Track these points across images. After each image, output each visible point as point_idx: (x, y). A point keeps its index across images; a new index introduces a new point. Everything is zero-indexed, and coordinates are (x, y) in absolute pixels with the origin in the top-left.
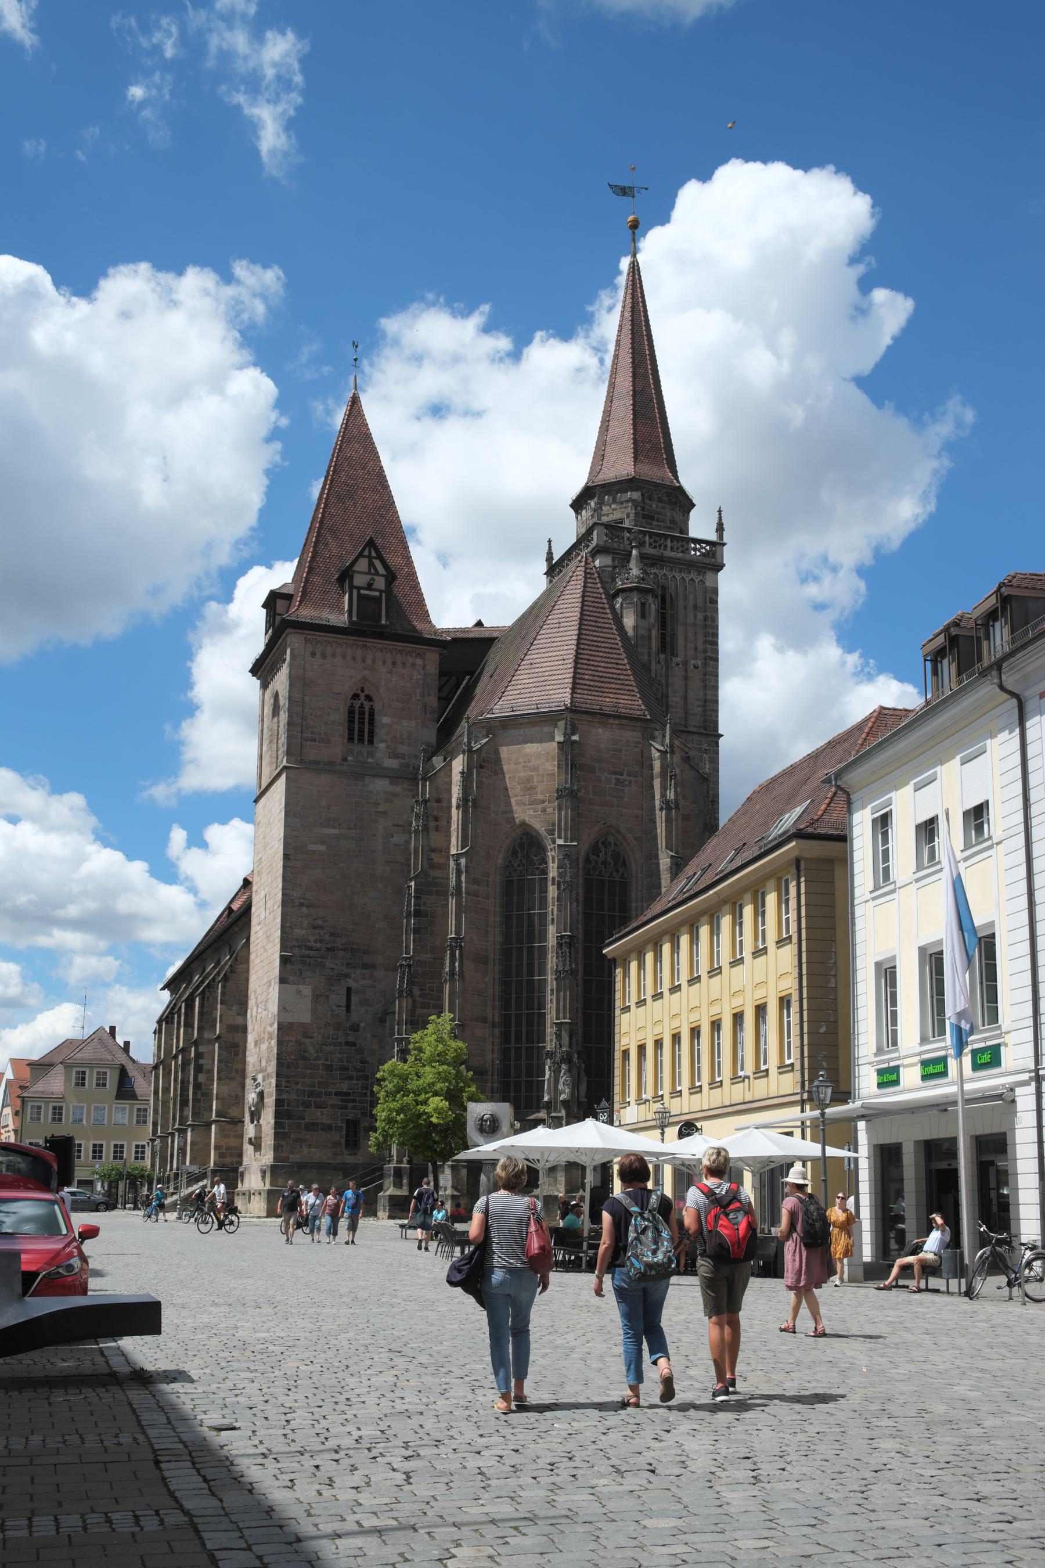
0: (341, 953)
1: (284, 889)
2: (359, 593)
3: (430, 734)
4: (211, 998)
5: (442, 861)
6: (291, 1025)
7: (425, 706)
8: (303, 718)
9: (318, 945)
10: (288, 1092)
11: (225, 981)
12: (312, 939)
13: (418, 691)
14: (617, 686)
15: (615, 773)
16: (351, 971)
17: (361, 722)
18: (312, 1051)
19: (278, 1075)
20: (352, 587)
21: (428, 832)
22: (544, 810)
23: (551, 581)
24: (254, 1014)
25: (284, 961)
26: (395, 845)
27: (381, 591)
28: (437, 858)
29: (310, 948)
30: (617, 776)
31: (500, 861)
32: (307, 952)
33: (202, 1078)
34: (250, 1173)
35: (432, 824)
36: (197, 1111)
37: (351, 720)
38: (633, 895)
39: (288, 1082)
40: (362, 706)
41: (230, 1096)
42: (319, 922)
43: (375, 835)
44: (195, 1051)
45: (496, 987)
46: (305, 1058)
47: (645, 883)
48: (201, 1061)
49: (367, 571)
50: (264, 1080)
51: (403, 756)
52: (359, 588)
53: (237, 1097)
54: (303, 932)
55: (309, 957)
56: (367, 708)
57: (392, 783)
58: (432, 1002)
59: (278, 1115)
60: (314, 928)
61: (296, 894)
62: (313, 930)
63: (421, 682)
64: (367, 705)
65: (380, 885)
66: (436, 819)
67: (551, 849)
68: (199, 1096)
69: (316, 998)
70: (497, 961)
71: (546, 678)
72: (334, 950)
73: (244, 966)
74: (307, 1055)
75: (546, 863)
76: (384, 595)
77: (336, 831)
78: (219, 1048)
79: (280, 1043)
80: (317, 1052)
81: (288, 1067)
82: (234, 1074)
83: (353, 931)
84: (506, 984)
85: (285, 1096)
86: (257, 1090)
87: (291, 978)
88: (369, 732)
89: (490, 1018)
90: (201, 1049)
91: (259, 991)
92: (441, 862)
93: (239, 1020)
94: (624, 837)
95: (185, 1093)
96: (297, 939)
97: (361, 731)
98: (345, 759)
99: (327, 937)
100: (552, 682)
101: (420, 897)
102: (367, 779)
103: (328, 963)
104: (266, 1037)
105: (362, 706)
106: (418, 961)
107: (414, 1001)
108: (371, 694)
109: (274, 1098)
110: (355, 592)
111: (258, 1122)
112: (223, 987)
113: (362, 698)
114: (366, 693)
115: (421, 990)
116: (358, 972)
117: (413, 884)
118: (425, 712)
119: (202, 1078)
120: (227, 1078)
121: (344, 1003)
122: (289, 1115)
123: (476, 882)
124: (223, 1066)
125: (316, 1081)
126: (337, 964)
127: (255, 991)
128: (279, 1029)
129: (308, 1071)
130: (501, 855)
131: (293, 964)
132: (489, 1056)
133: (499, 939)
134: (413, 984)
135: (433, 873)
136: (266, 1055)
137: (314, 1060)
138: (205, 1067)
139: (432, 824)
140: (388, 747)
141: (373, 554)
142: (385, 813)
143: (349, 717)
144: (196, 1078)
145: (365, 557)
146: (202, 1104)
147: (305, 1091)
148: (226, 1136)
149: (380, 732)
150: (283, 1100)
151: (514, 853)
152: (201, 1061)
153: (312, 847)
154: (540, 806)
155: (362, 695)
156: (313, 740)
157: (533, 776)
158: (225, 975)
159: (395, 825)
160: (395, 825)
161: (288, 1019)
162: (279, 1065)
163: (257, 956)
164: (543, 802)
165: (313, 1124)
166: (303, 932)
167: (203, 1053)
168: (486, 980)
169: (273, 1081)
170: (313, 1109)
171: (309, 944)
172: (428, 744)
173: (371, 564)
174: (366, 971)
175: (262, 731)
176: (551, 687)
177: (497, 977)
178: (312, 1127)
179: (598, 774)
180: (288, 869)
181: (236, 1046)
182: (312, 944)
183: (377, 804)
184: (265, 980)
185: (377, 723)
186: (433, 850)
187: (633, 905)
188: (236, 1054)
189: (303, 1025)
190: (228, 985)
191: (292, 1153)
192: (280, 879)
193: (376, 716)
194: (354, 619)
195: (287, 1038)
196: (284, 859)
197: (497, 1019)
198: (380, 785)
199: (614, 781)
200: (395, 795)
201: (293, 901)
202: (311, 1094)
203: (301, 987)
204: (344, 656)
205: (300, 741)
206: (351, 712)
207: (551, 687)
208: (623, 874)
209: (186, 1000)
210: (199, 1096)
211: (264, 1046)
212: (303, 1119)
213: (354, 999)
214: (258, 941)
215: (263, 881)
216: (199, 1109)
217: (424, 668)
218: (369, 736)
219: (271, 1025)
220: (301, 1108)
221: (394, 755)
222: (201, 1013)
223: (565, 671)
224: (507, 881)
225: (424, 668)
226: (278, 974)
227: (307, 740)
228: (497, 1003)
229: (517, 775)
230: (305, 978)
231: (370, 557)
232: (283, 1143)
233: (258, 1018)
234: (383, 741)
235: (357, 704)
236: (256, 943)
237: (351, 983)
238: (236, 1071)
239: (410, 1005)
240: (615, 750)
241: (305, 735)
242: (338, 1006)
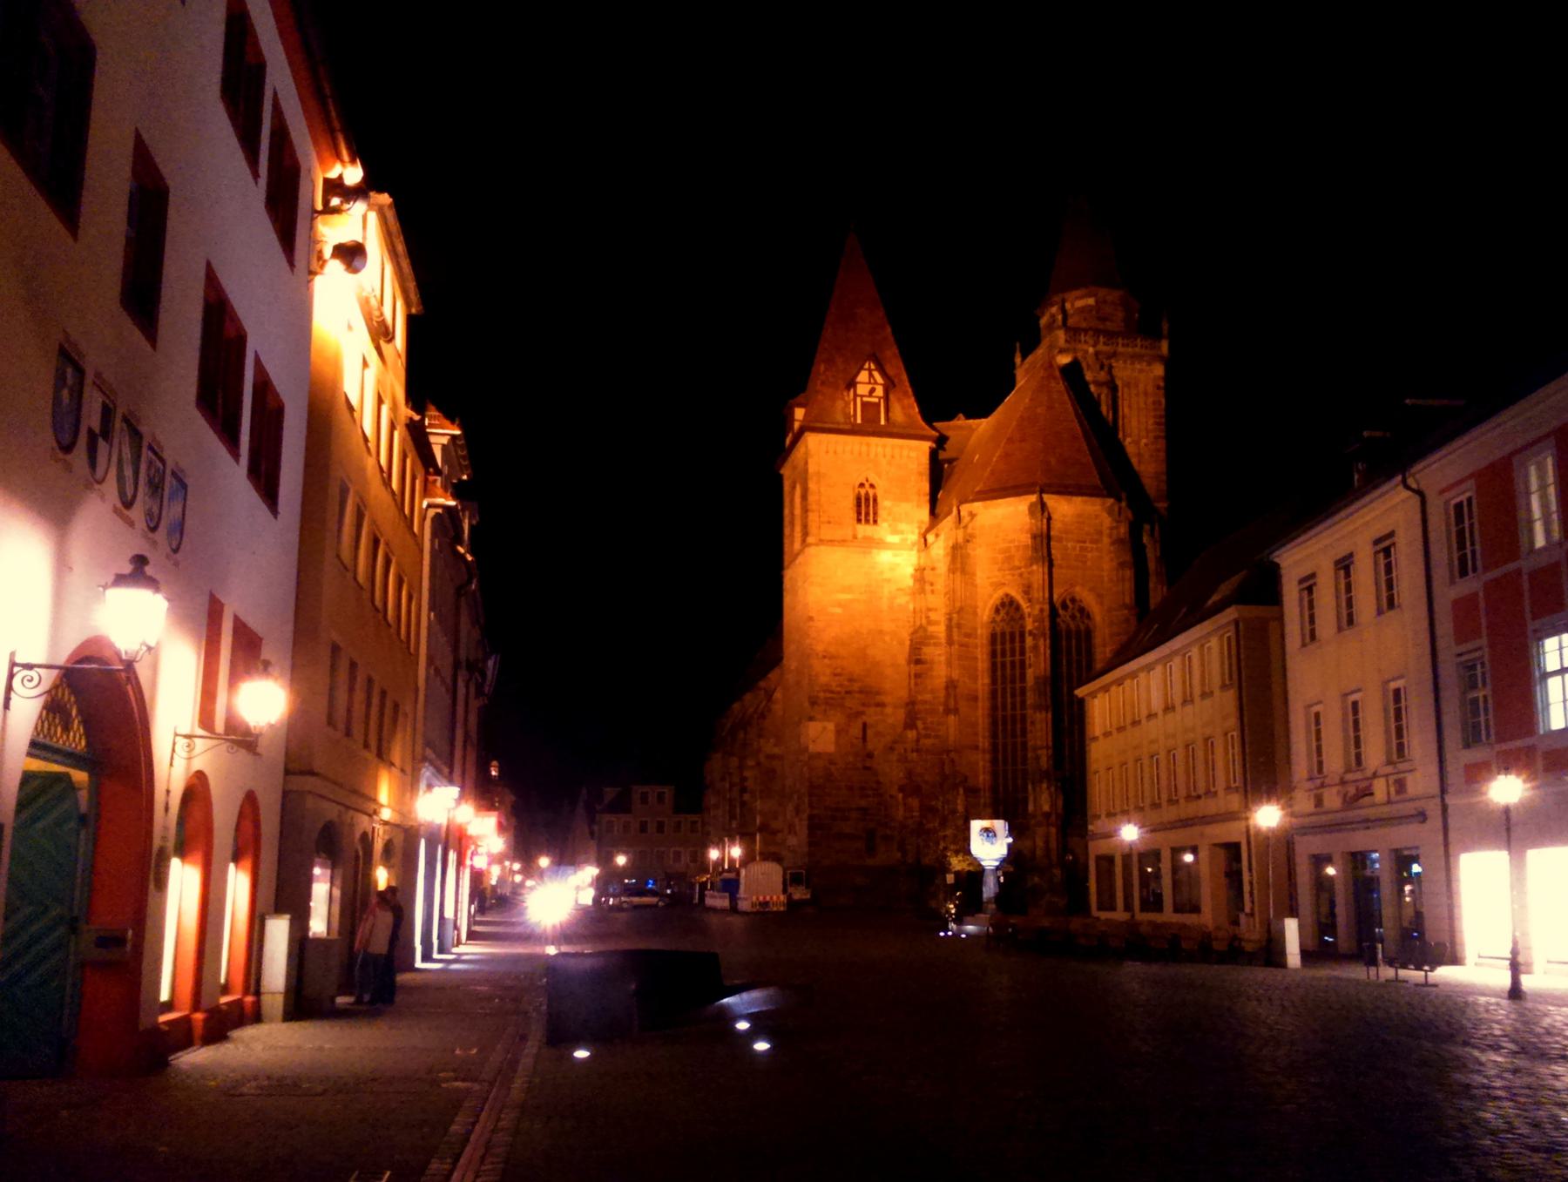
0: (857, 695)
2: (862, 400)
9: (839, 689)
12: (834, 684)
15: (1079, 541)
17: (867, 506)
20: (856, 395)
21: (925, 594)
22: (1021, 575)
27: (880, 398)
29: (832, 692)
30: (1082, 545)
33: (746, 797)
35: (928, 588)
37: (859, 505)
40: (867, 494)
42: (839, 671)
49: (867, 380)
52: (862, 396)
55: (832, 698)
56: (871, 495)
58: (933, 734)
66: (932, 584)
69: (839, 732)
76: (882, 401)
85: (816, 812)
99: (846, 683)
103: (848, 703)
105: (867, 494)
108: (874, 483)
110: (859, 400)
114: (870, 482)
115: (924, 724)
119: (746, 797)
132: (981, 778)
133: (987, 681)
141: (873, 367)
145: (865, 370)
151: (997, 611)
154: (1019, 571)
155: (867, 485)
156: (829, 522)
164: (1019, 568)
172: (922, 522)
173: (871, 375)
179: (1065, 543)
186: (929, 610)
194: (859, 421)
199: (1078, 549)
203: (826, 724)
204: (852, 453)
206: (858, 499)
213: (870, 733)
227: (823, 523)
231: (870, 370)
235: (863, 492)
237: (865, 718)
240: (1078, 522)
242: (857, 738)
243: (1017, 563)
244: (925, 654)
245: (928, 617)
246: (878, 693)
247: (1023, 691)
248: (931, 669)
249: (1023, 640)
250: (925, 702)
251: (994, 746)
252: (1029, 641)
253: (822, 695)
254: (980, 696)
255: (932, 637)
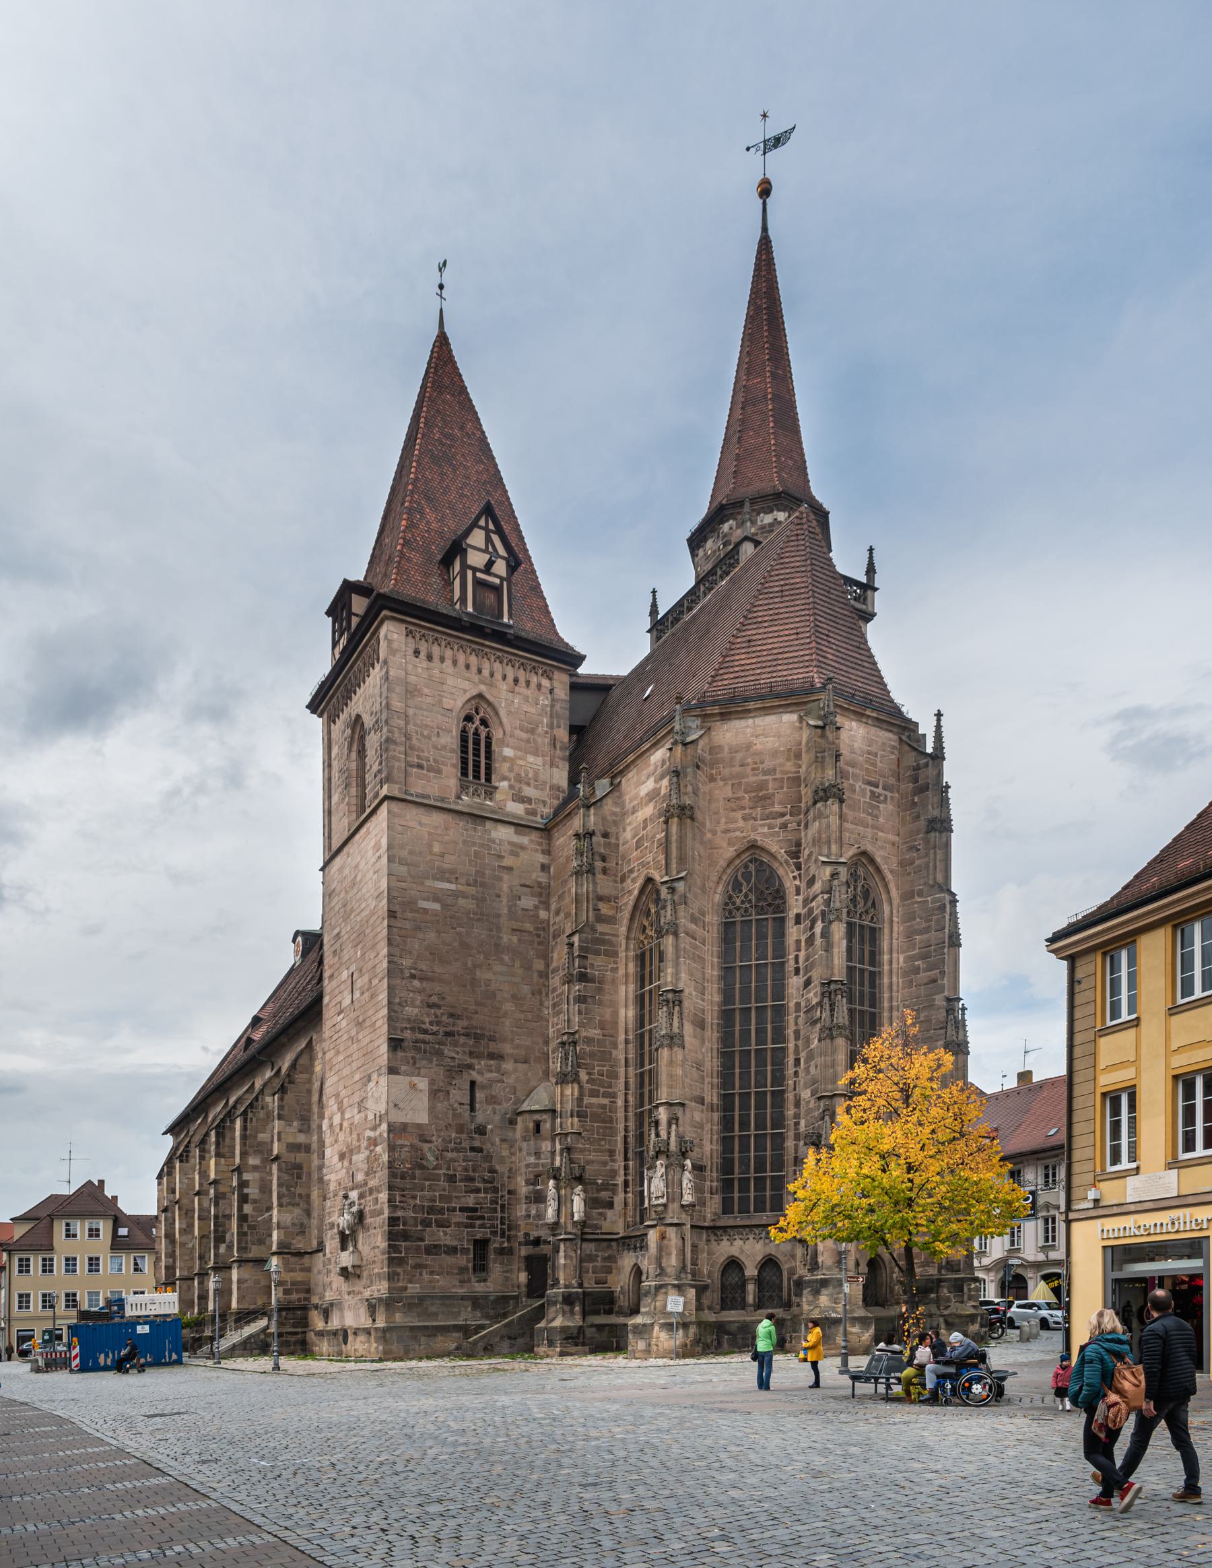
0: (462, 1039)
1: (390, 955)
3: (560, 776)
4: (254, 1120)
5: (611, 913)
6: (404, 1127)
7: (555, 739)
8: (408, 737)
9: (435, 1028)
10: (403, 1208)
11: (283, 1093)
12: (427, 1020)
13: (545, 720)
14: (864, 675)
16: (475, 1061)
17: (477, 753)
18: (432, 1159)
19: (390, 1188)
21: (594, 874)
22: (784, 826)
23: (659, 638)
24: (337, 1120)
25: (395, 1044)
26: (523, 909)
28: (605, 909)
29: (425, 1032)
31: (717, 898)
32: (422, 1036)
33: (247, 1209)
34: (341, 1310)
35: (599, 864)
36: (244, 1245)
38: (886, 946)
39: (403, 1196)
40: (476, 733)
41: (294, 1224)
42: (434, 999)
43: (498, 896)
44: (239, 1178)
45: (715, 1060)
46: (423, 1167)
47: (901, 928)
48: (246, 1191)
50: (361, 1196)
51: (529, 801)
53: (302, 1225)
54: (416, 1011)
55: (424, 1042)
57: (516, 833)
59: (392, 1236)
60: (429, 1006)
61: (406, 962)
62: (427, 1009)
63: (548, 709)
64: (483, 732)
65: (506, 958)
66: (604, 859)
67: (795, 878)
68: (245, 1229)
69: (434, 1093)
70: (715, 1027)
71: (775, 657)
72: (454, 1035)
73: (305, 1076)
74: (424, 1162)
75: (783, 898)
77: (453, 887)
78: (279, 1170)
79: (391, 1148)
80: (437, 1159)
81: (403, 1178)
82: (297, 1200)
83: (476, 1013)
84: (726, 1057)
85: (400, 1214)
86: (355, 1209)
87: (403, 1068)
88: (486, 769)
89: (708, 1099)
90: (246, 1177)
91: (343, 1093)
92: (610, 914)
93: (301, 1138)
94: (878, 870)
95: (221, 1229)
96: (409, 1020)
97: (477, 765)
98: (459, 798)
99: (445, 1019)
100: (786, 661)
101: (586, 958)
102: (489, 824)
104: (364, 1144)
105: (476, 733)
106: (585, 1037)
107: (581, 1087)
109: (386, 1215)
111: (355, 1246)
112: (281, 1099)
113: (477, 723)
116: (483, 1062)
117: (576, 939)
118: (555, 747)
119: (247, 1209)
120: (289, 1204)
121: (467, 1100)
122: (406, 1236)
123: (694, 920)
124: (284, 1190)
125: (437, 1194)
126: (458, 1053)
127: (337, 1096)
128: (389, 1131)
129: (427, 1183)
130: (720, 889)
131: (404, 1051)
133: (717, 998)
134: (579, 1066)
135: (601, 928)
136: (365, 1166)
137: (434, 1169)
138: (251, 1197)
139: (599, 864)
140: (511, 787)
142: (509, 869)
143: (462, 746)
144: (240, 1209)
146: (249, 1238)
147: (423, 1206)
148: (292, 1270)
149: (501, 767)
150: (398, 1218)
151: (737, 886)
152: (246, 1191)
153: (423, 904)
156: (420, 766)
157: (767, 781)
158: (282, 1085)
159: (521, 885)
160: (521, 885)
161: (399, 1118)
162: (392, 1174)
163: (338, 1053)
165: (435, 1246)
166: (416, 1011)
167: (247, 1181)
168: (704, 1050)
169: (383, 1196)
170: (434, 1228)
171: (423, 1026)
174: (492, 1062)
175: (330, 779)
176: (785, 667)
177: (715, 1047)
178: (433, 1250)
180: (395, 930)
181: (299, 1167)
182: (427, 1026)
183: (501, 857)
184: (357, 1077)
185: (495, 756)
186: (600, 898)
187: (886, 957)
188: (299, 1177)
189: (419, 1126)
190: (286, 1097)
191: (411, 1283)
192: (384, 943)
193: (494, 747)
195: (400, 1142)
196: (389, 916)
197: (715, 1101)
198: (504, 834)
200: (522, 848)
201: (402, 971)
202: (431, 1210)
203: (415, 1080)
205: (403, 765)
207: (785, 667)
208: (872, 918)
209: (216, 1127)
210: (245, 1229)
211: (360, 1158)
212: (422, 1240)
214: (340, 1034)
215: (346, 958)
216: (246, 1243)
217: (551, 691)
218: (486, 774)
219: (374, 1128)
220: (420, 1228)
221: (519, 798)
222: (244, 1137)
223: (802, 647)
224: (726, 923)
225: (551, 691)
226: (386, 1062)
227: (412, 766)
228: (715, 1081)
229: (744, 781)
230: (419, 1068)
232: (399, 1270)
233: (345, 1124)
234: (504, 778)
236: (334, 1038)
237: (474, 1075)
238: (300, 1196)
239: (576, 1093)
241: (409, 759)
242: (460, 1104)
243: (778, 808)
244: (592, 965)
245: (596, 910)
246: (492, 1039)
247: (780, 1011)
248: (600, 990)
249: (781, 934)
250: (589, 1041)
251: (727, 1102)
252: (793, 933)
253: (408, 1034)
254: (709, 1020)
255: (603, 942)
